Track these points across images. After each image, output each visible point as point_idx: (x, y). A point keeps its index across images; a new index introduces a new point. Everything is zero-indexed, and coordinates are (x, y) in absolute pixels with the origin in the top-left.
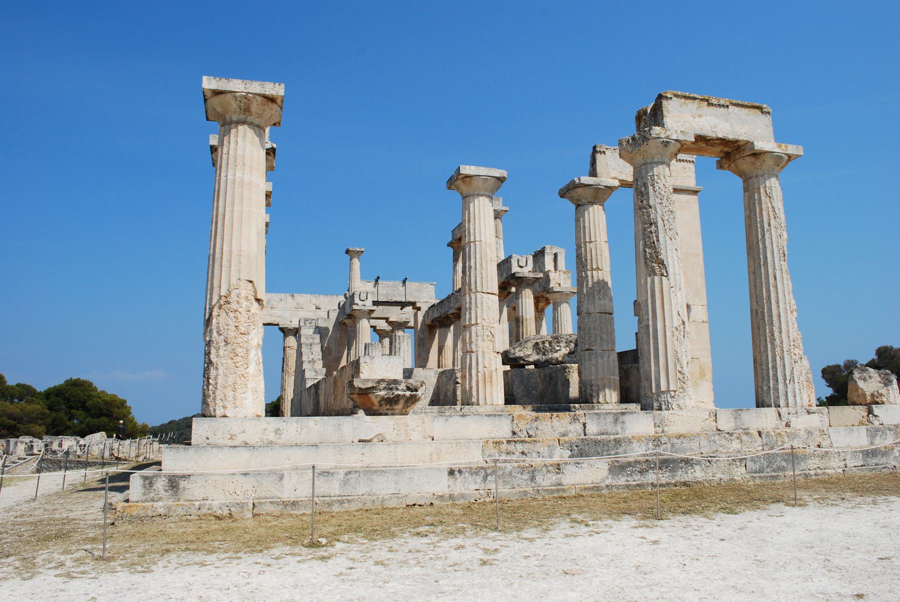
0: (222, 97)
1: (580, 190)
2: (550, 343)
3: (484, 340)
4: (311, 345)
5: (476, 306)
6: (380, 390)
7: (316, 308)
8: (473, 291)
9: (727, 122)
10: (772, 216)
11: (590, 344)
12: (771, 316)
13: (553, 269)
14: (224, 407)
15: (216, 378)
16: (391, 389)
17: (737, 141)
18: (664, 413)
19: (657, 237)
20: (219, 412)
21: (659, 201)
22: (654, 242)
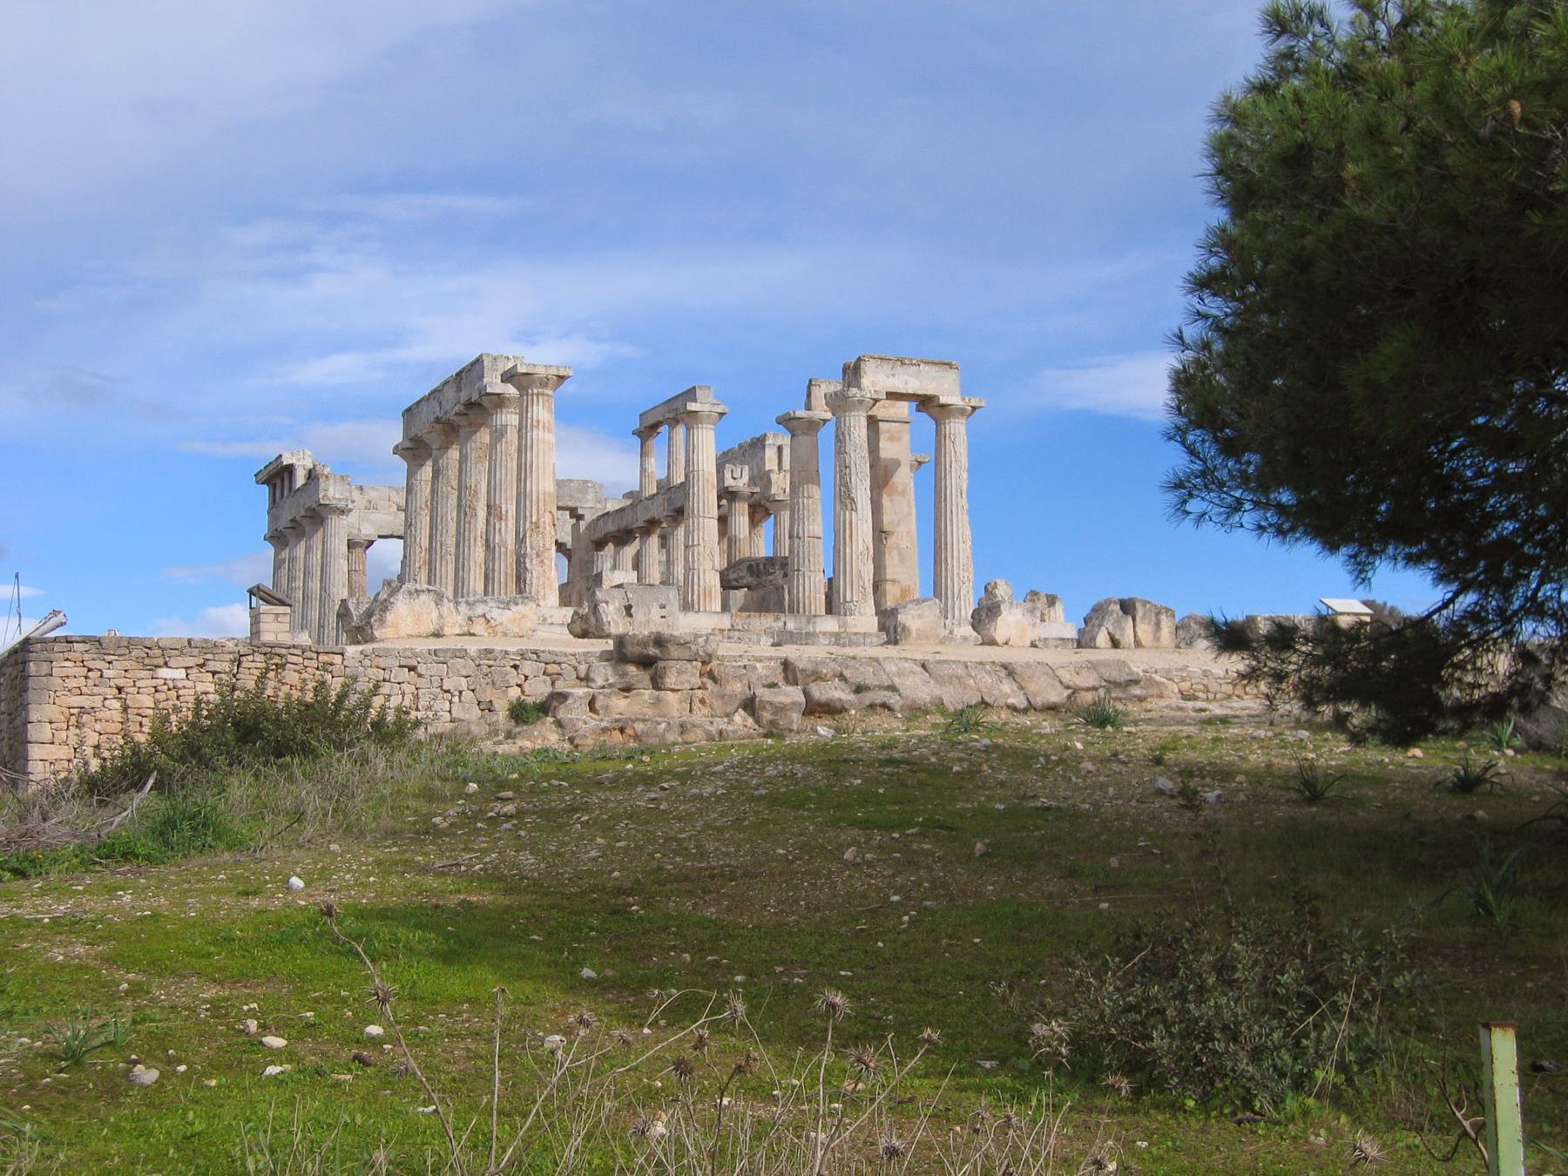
1: (795, 422)
2: (765, 565)
9: (917, 378)
12: (946, 544)
13: (776, 468)
18: (849, 618)
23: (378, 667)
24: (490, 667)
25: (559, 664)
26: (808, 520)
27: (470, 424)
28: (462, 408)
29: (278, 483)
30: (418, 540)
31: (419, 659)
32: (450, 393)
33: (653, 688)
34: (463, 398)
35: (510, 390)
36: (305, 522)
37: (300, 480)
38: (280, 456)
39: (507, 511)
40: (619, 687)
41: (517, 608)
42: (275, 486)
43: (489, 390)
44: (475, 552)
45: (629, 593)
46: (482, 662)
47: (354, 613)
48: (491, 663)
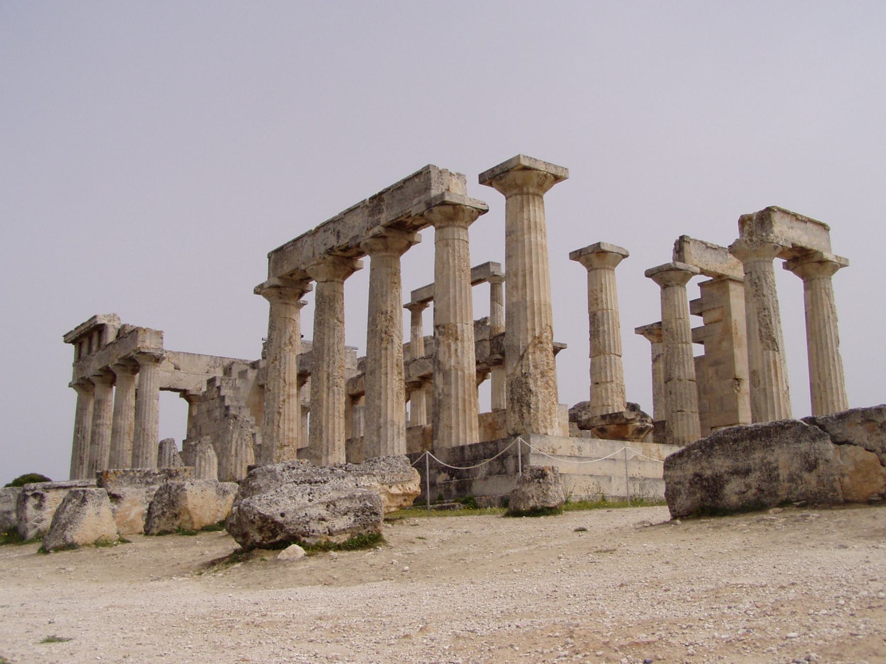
1: (672, 273)
3: (618, 396)
4: (240, 408)
5: (611, 366)
6: (637, 422)
7: (175, 369)
8: (608, 352)
10: (830, 312)
11: (682, 406)
14: (545, 427)
15: (536, 404)
16: (643, 421)
17: (810, 250)
19: (770, 320)
20: (542, 431)
21: (770, 292)
22: (768, 324)
26: (688, 364)
27: (387, 249)
28: (382, 229)
30: (282, 375)
34: (386, 217)
37: (111, 336)
38: (95, 317)
39: (463, 331)
43: (447, 198)
44: (392, 379)
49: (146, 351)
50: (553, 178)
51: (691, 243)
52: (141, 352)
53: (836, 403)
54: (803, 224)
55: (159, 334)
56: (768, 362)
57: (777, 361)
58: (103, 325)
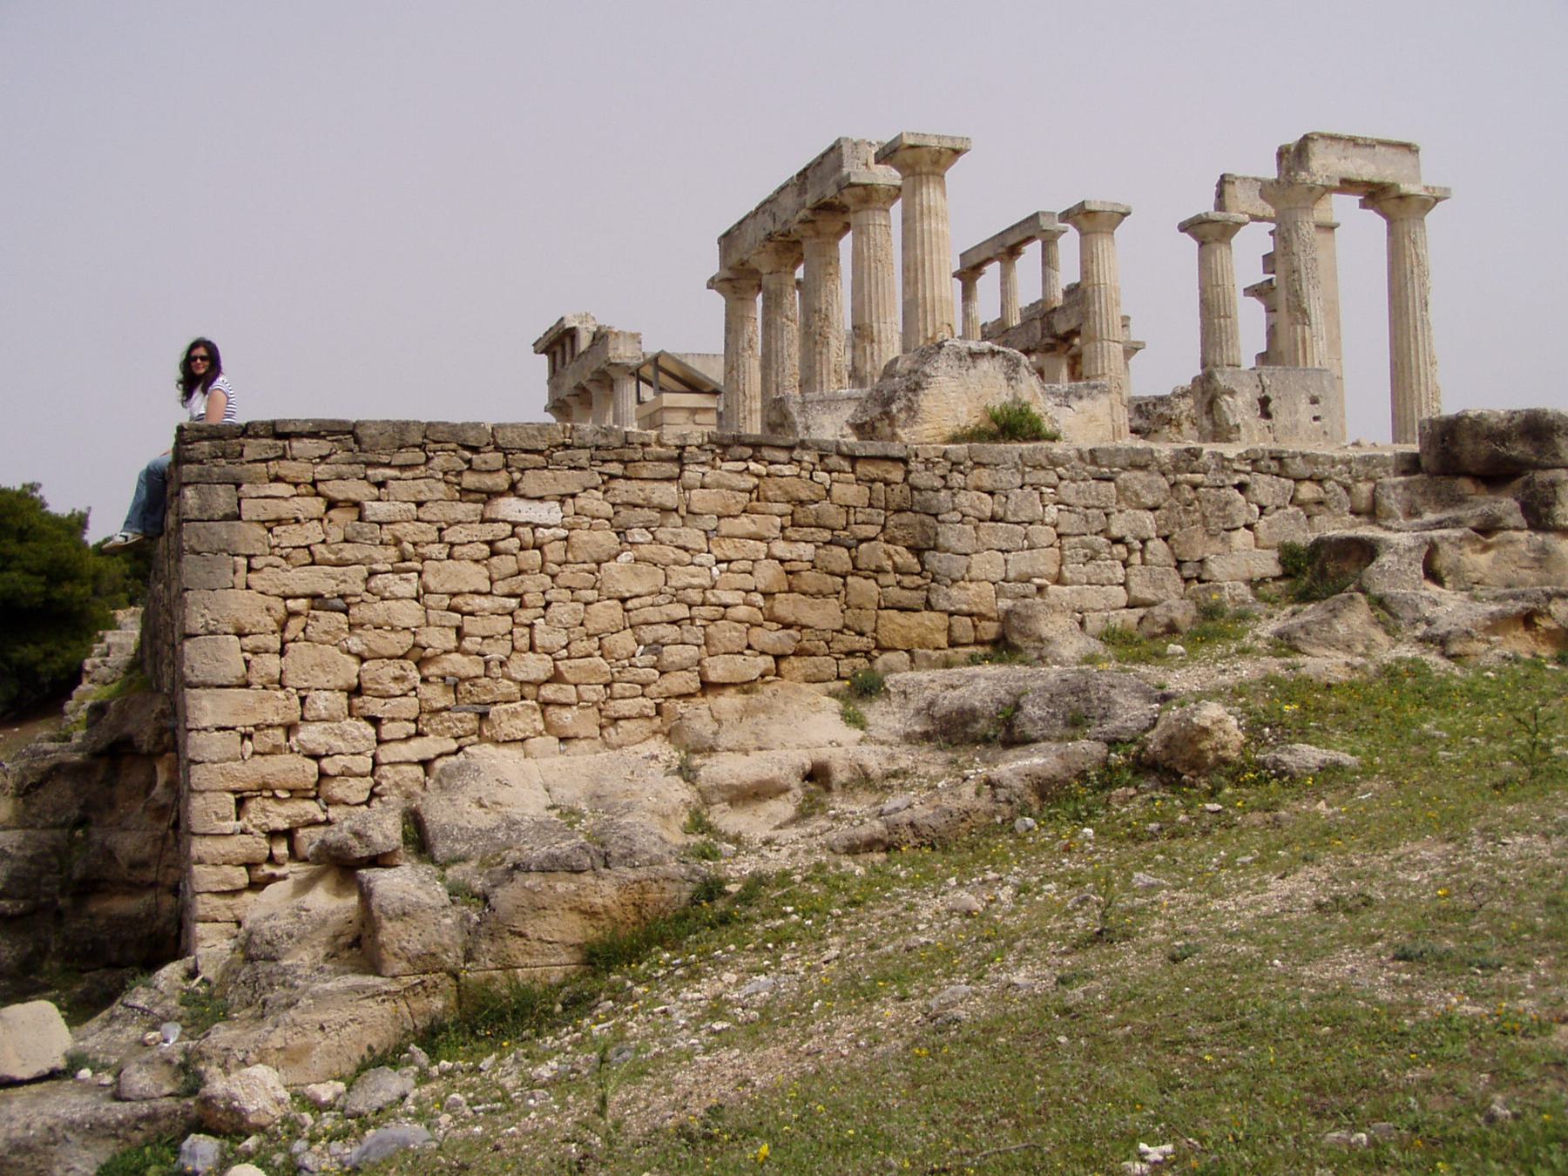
0: (917, 150)
1: (1207, 227)
23: (978, 489)
24: (1195, 487)
25: (1320, 482)
27: (818, 234)
29: (558, 349)
31: (1060, 470)
32: (789, 201)
33: (1531, 527)
34: (810, 199)
35: (887, 175)
36: (592, 388)
37: (584, 342)
38: (562, 319)
39: (879, 332)
40: (1474, 523)
41: (1080, 404)
42: (554, 354)
43: (853, 180)
45: (1264, 378)
46: (1180, 477)
47: (798, 419)
48: (1198, 478)
49: (618, 361)
50: (950, 152)
51: (1237, 183)
52: (611, 364)
53: (1415, 387)
54: (1368, 150)
55: (636, 337)
56: (1296, 340)
57: (1307, 336)
58: (574, 329)
